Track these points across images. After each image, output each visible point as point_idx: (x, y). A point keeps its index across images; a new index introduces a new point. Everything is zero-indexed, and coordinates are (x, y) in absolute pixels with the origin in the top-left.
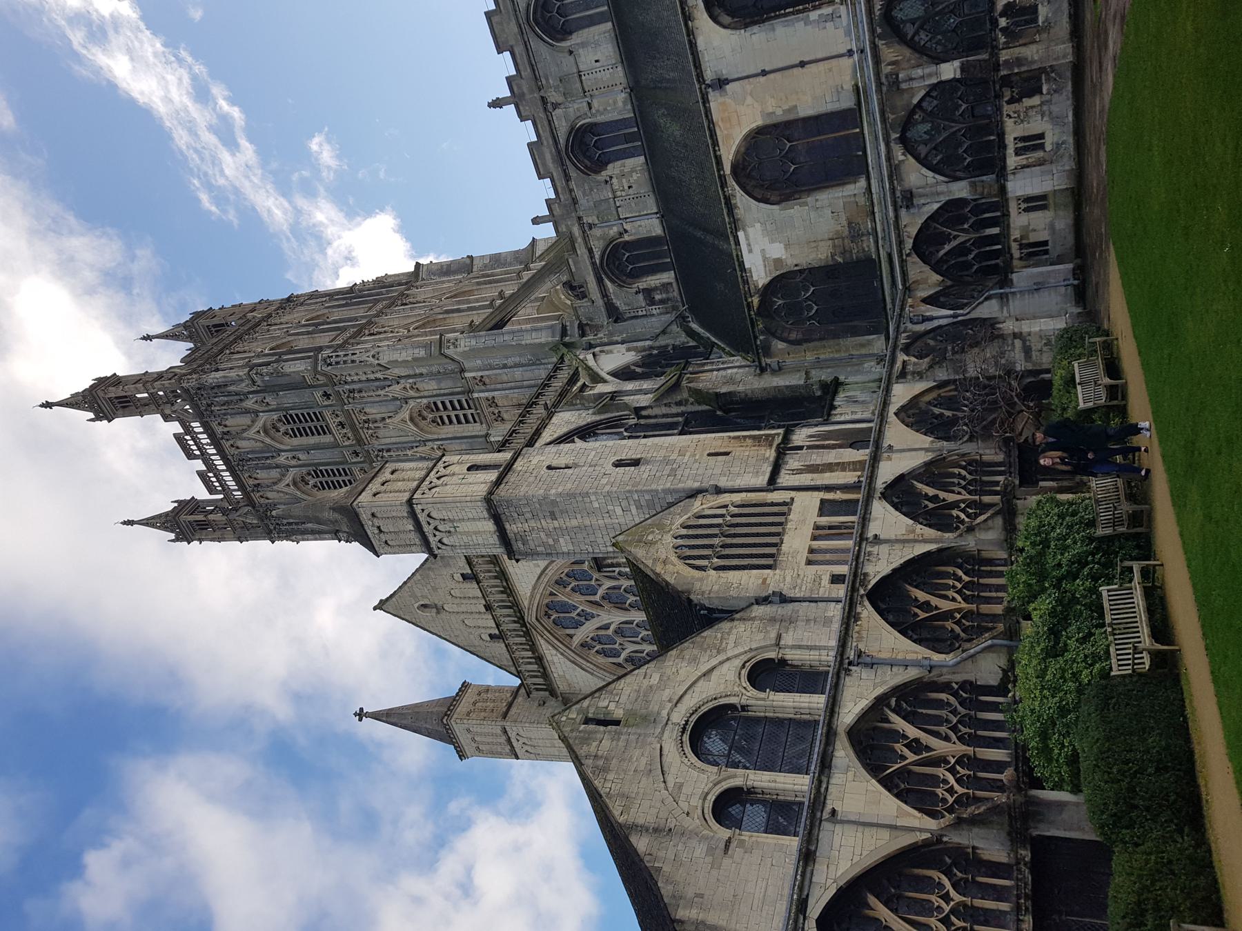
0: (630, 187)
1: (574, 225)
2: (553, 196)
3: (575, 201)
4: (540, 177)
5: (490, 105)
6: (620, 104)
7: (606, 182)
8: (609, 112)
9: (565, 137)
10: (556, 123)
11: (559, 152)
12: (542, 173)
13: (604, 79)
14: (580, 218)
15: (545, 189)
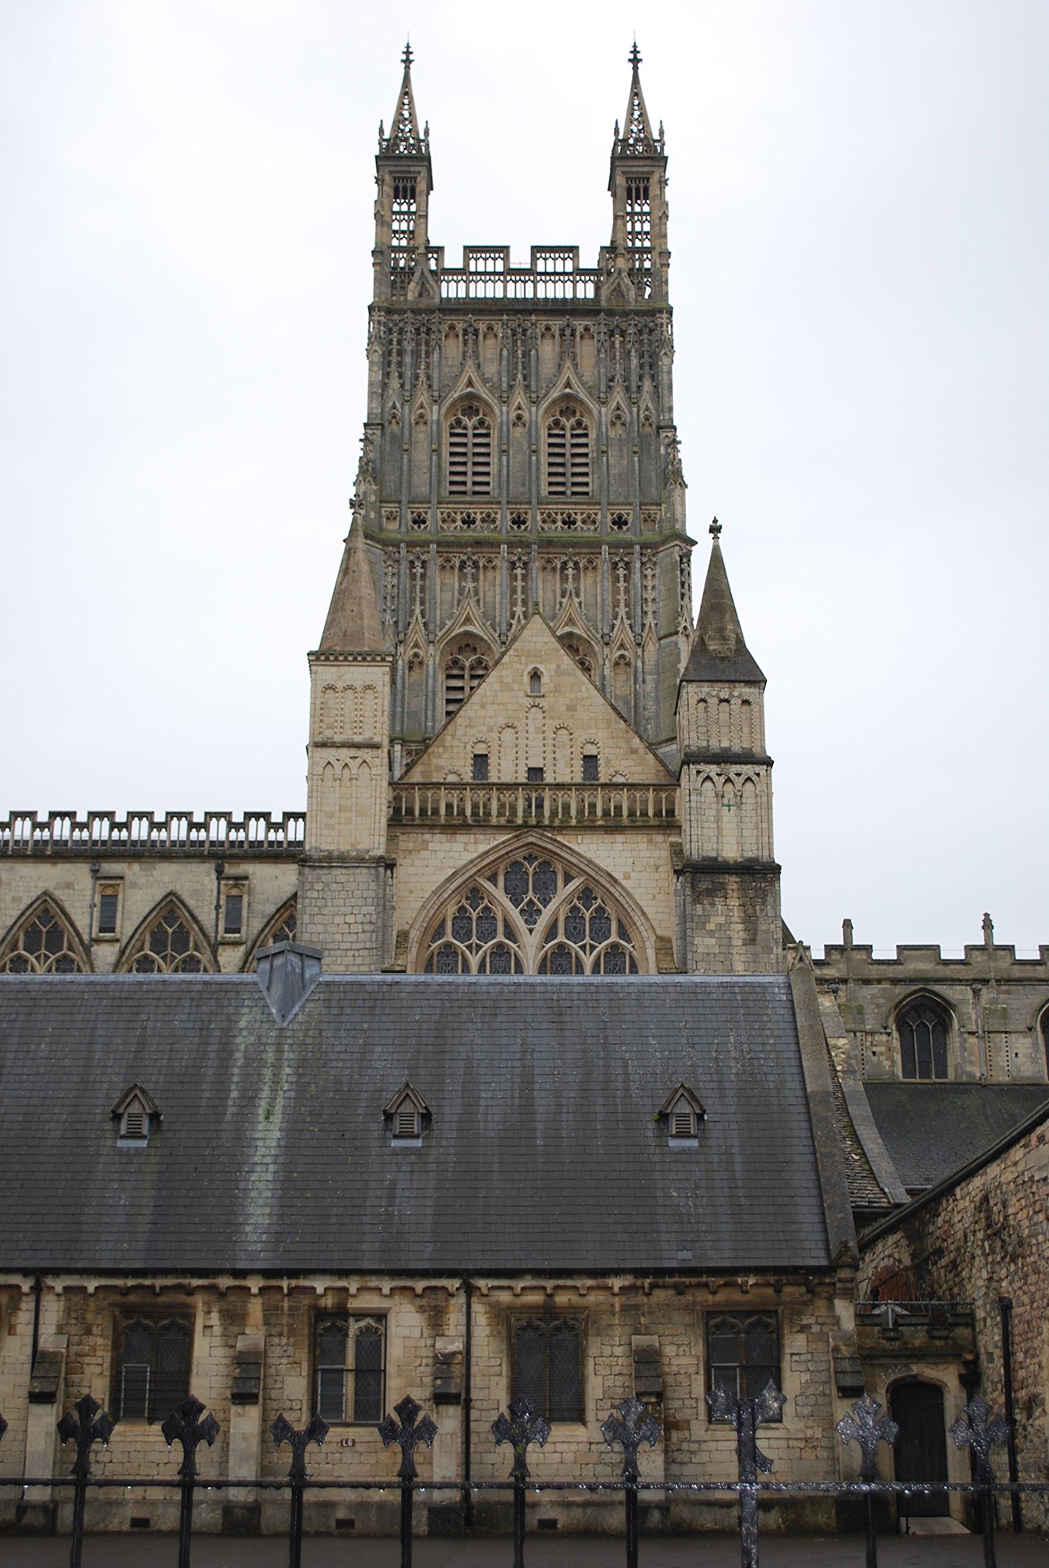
0: (874, 1053)
1: (838, 970)
2: (875, 956)
3: (867, 982)
4: (901, 949)
5: (987, 915)
6: (969, 1068)
7: (885, 1028)
8: (962, 1053)
9: (941, 992)
10: (958, 987)
11: (927, 980)
12: (906, 952)
13: (999, 1059)
14: (845, 981)
15: (886, 952)
